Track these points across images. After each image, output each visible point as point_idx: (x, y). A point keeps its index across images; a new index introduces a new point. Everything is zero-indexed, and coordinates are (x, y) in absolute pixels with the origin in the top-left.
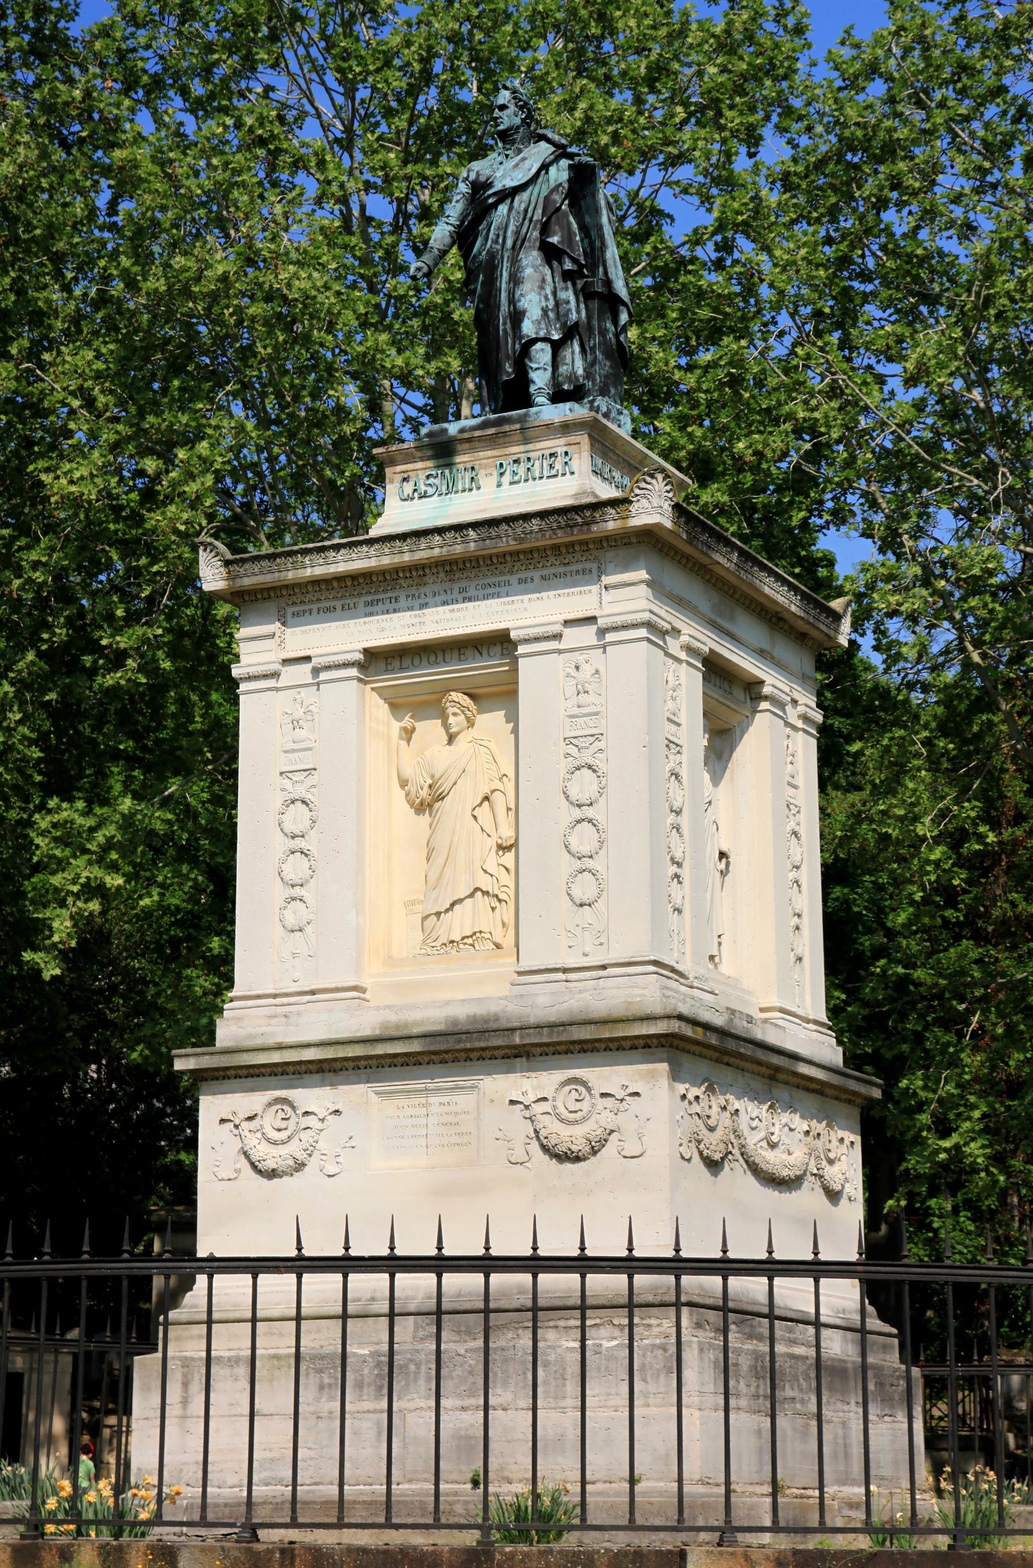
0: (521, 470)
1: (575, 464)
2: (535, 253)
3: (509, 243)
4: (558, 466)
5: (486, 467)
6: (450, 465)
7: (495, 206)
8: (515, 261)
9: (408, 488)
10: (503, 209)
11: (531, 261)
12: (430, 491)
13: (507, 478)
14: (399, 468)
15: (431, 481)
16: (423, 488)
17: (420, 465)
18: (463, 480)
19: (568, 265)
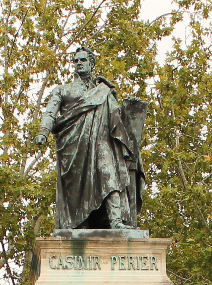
0: (126, 263)
1: (158, 265)
2: (106, 143)
3: (95, 134)
4: (148, 265)
5: (104, 258)
6: (81, 253)
7: (86, 113)
8: (97, 145)
9: (55, 263)
10: (90, 115)
11: (105, 148)
12: (69, 266)
13: (117, 267)
14: (49, 250)
15: (70, 260)
16: (65, 264)
17: (62, 251)
18: (91, 264)
19: (126, 154)
